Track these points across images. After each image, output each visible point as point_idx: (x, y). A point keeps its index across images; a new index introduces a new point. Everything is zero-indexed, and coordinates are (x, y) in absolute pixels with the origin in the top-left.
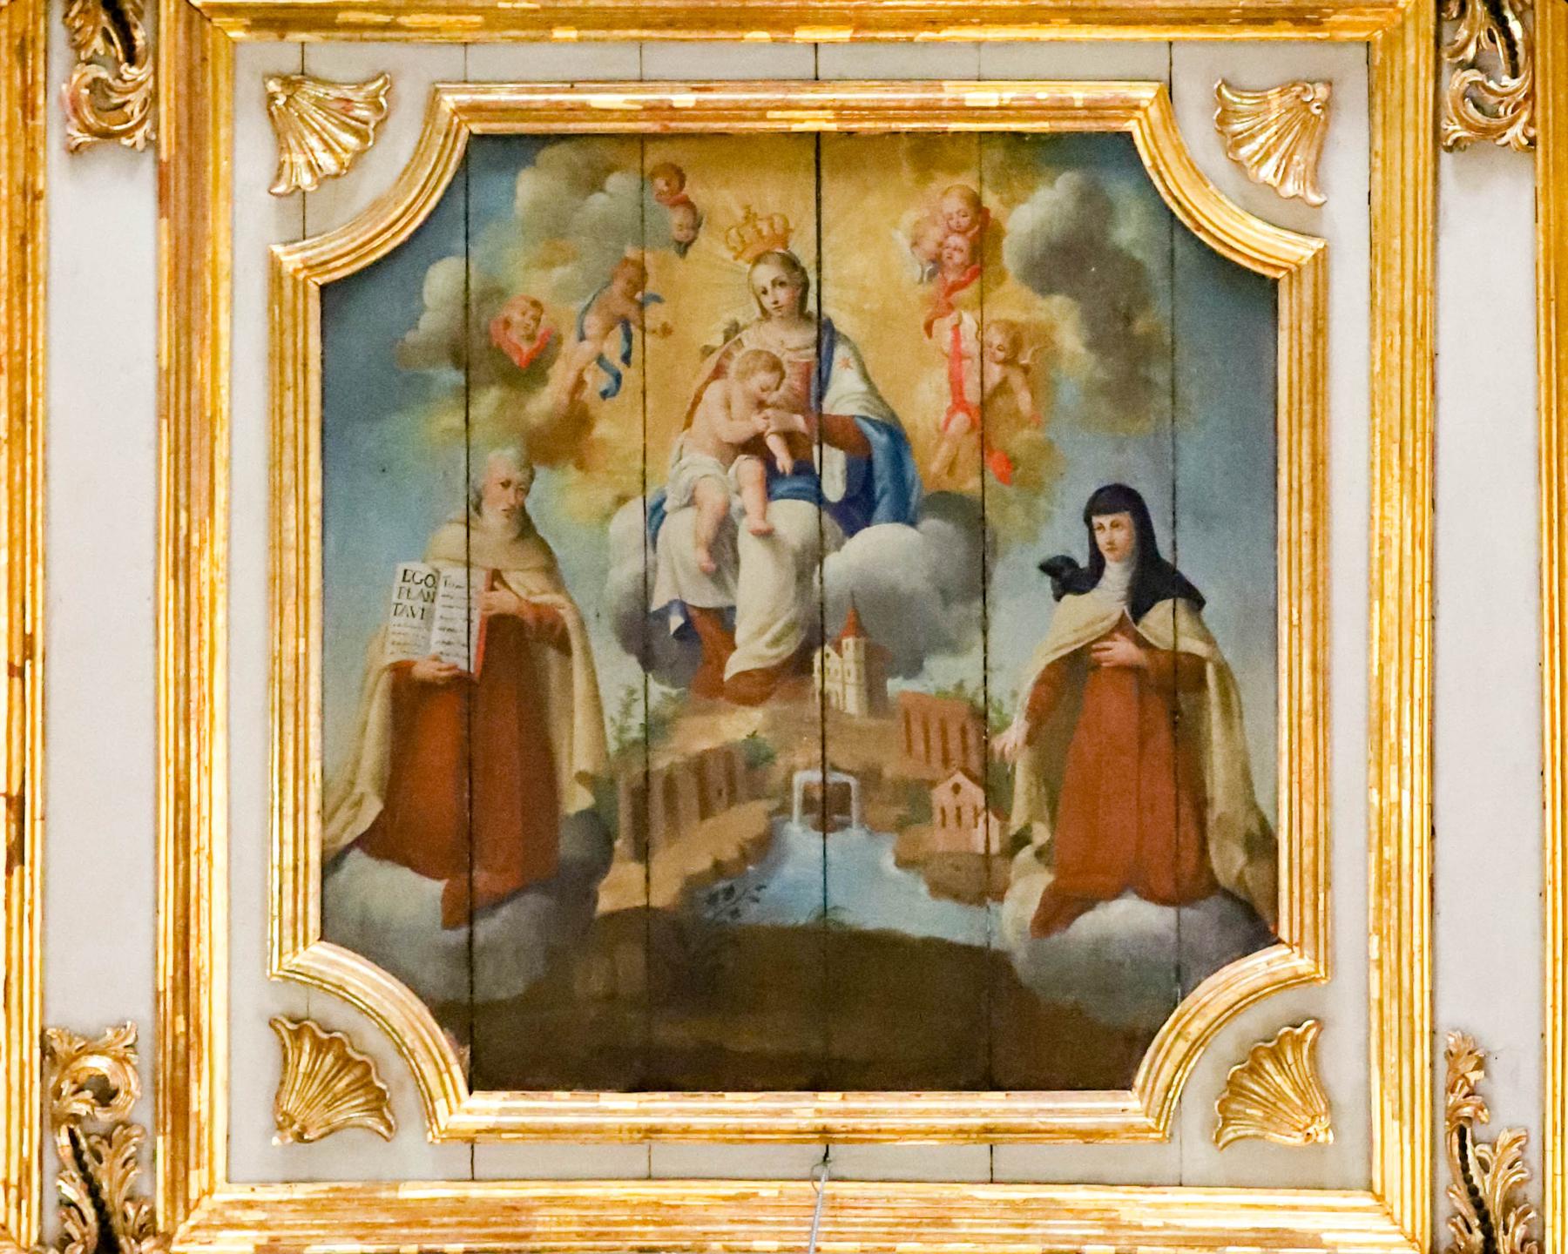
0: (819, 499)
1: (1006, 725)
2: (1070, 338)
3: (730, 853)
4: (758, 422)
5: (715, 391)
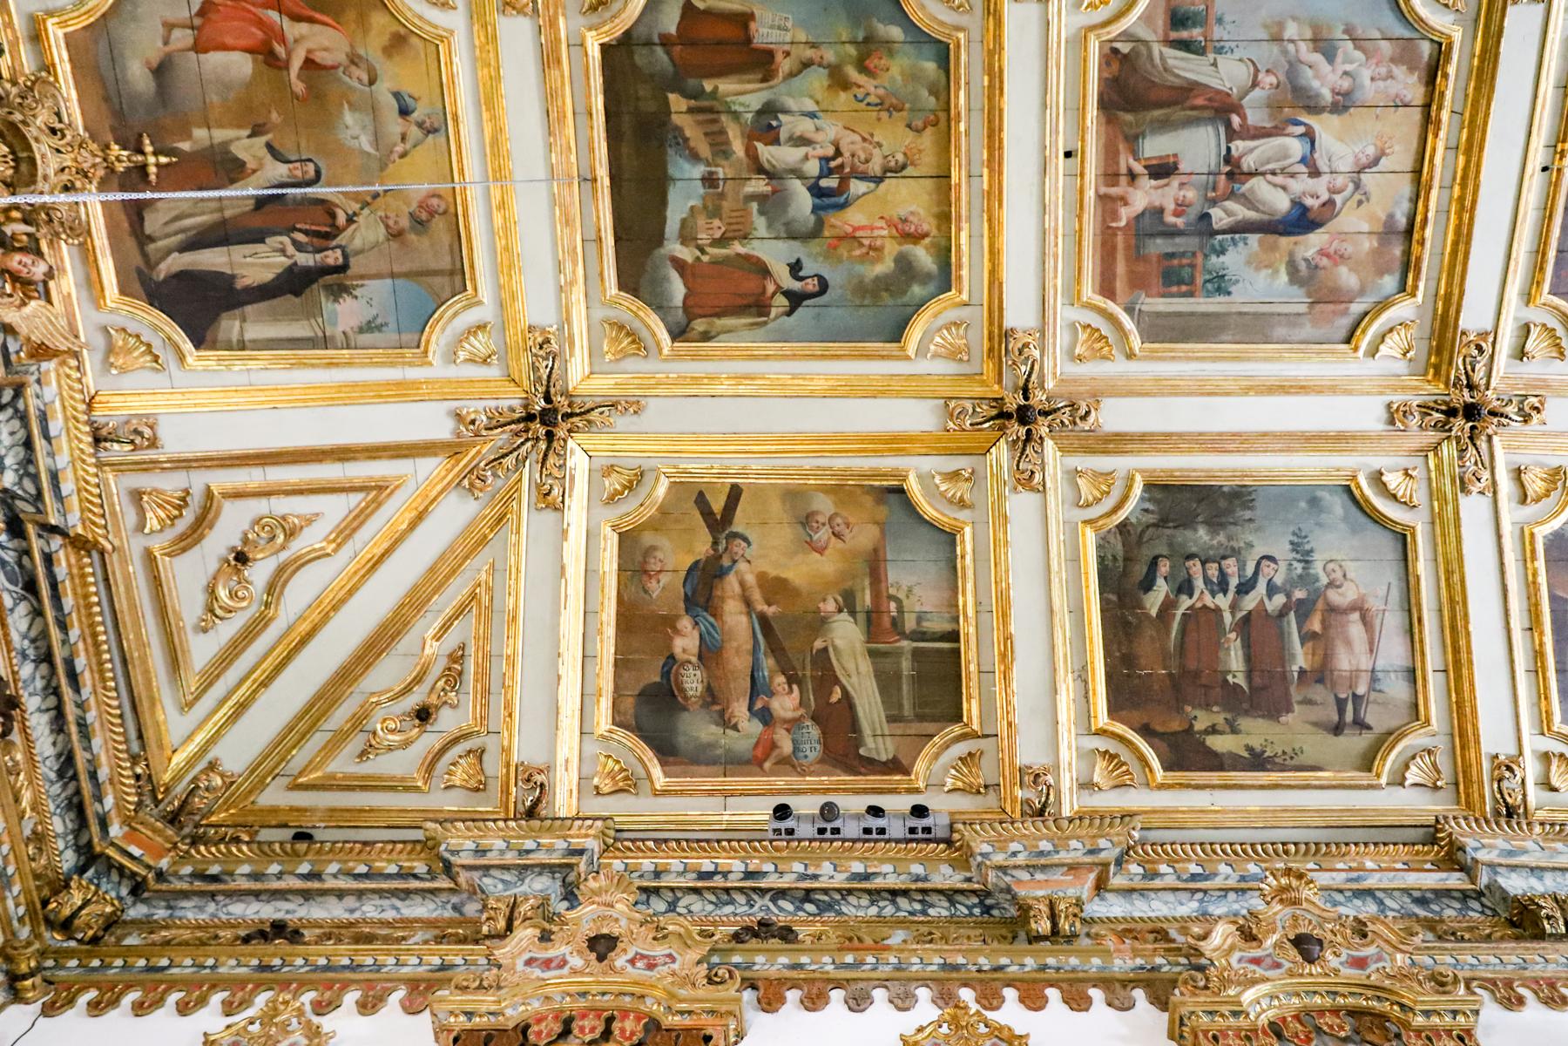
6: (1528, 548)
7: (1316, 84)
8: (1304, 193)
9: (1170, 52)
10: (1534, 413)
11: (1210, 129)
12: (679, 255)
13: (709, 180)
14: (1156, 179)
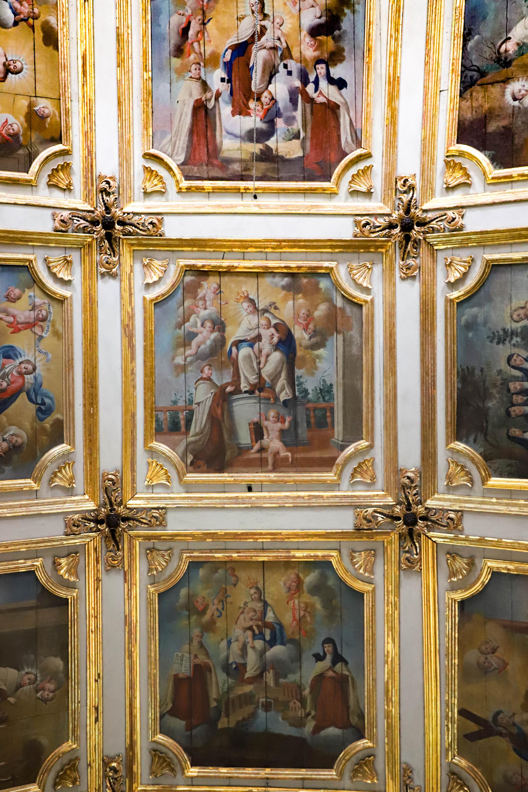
0: (264, 639)
1: (305, 689)
2: (318, 606)
3: (246, 716)
4: (251, 623)
5: (242, 617)
6: (502, 180)
7: (208, 342)
8: (271, 343)
9: (192, 431)
10: (408, 184)
11: (234, 404)
12: (311, 729)
13: (267, 707)
14: (264, 435)
